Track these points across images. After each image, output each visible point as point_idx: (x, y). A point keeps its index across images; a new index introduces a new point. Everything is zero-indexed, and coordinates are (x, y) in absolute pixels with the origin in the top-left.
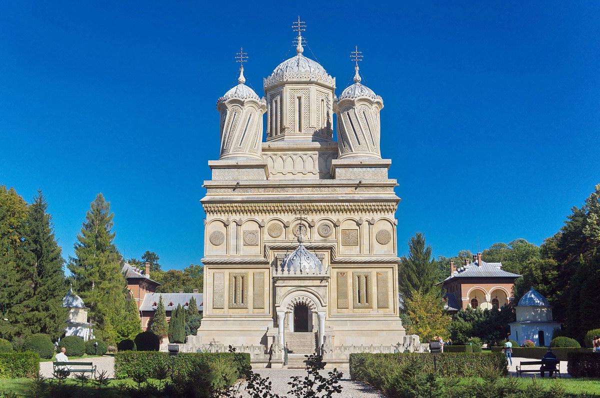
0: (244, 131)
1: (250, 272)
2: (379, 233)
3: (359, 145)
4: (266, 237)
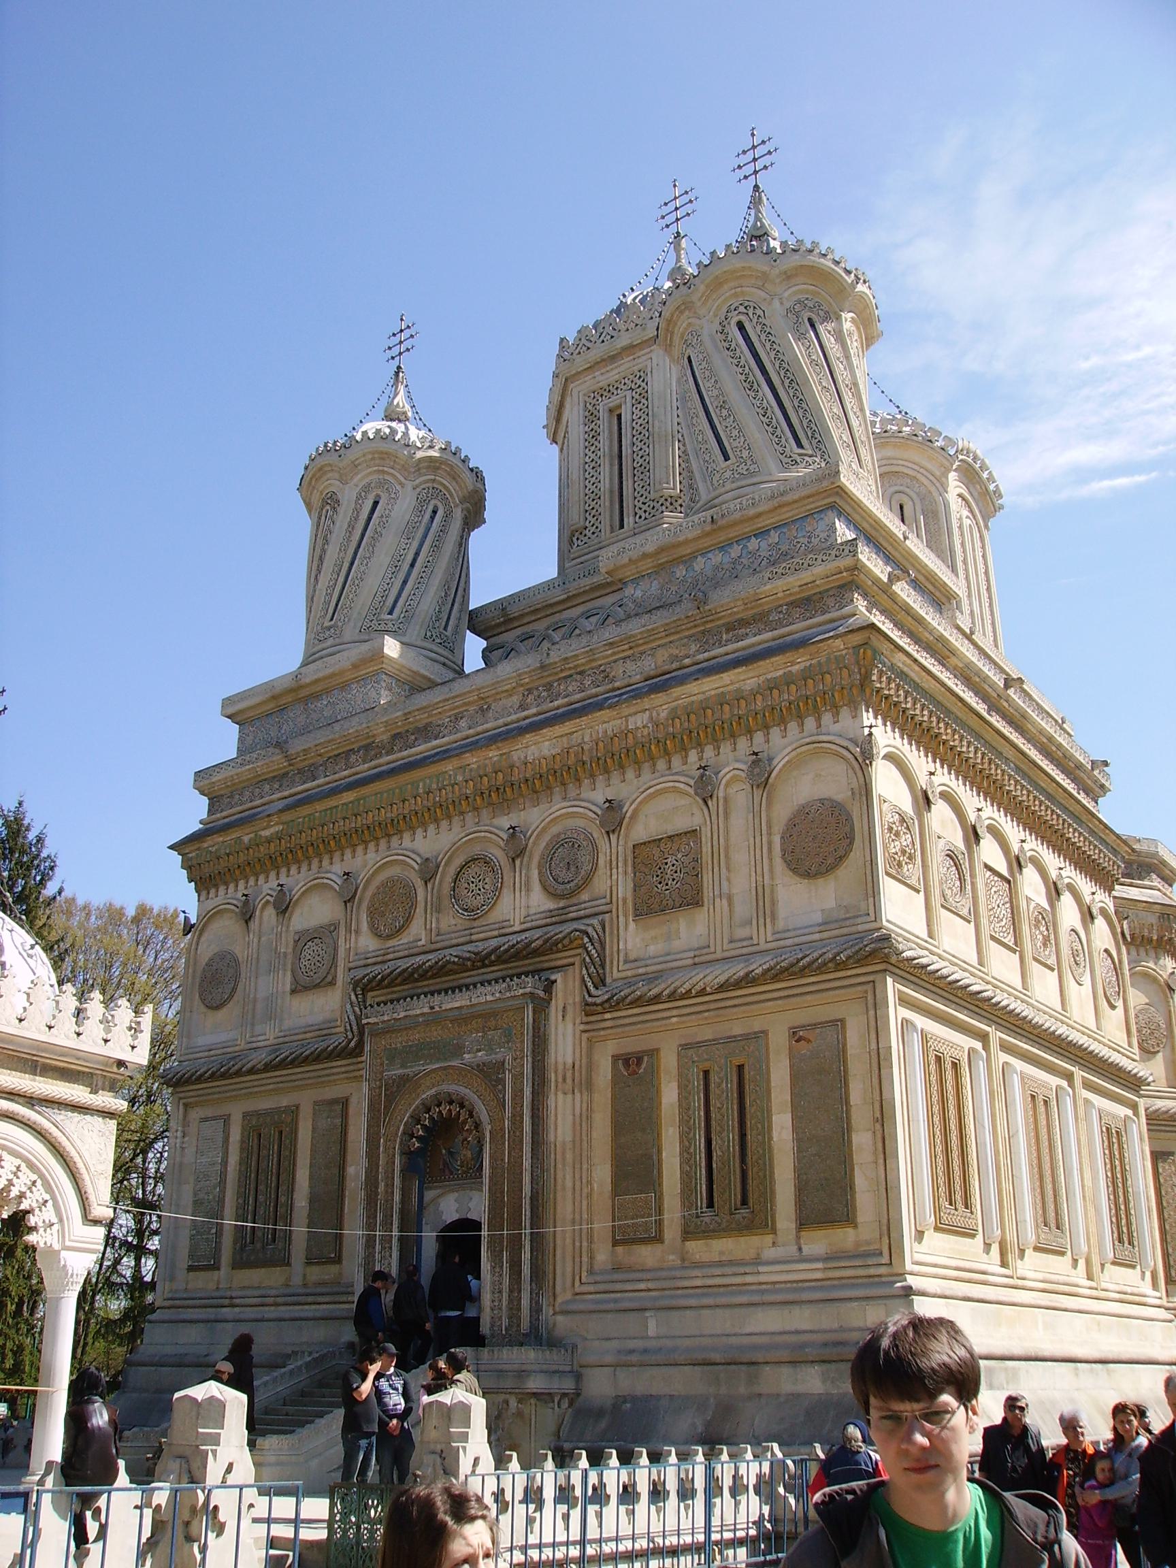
1: (306, 1100)
2: (792, 824)
3: (726, 458)
4: (367, 942)
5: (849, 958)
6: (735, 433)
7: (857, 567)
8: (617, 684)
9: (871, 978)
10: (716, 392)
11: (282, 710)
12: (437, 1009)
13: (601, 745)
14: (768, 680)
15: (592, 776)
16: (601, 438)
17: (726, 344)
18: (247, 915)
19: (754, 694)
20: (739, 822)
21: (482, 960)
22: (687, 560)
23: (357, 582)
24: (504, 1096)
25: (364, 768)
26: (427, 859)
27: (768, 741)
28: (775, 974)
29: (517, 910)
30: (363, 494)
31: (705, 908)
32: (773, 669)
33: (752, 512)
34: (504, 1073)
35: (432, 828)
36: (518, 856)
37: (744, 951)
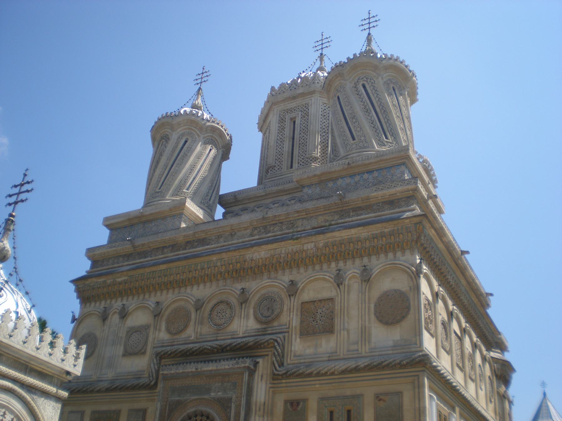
0: (169, 166)
3: (354, 139)
4: (163, 335)
5: (407, 363)
6: (359, 129)
7: (416, 190)
8: (299, 229)
9: (417, 373)
10: (350, 112)
11: (132, 225)
12: (199, 370)
13: (289, 255)
14: (373, 234)
15: (284, 269)
16: (286, 130)
17: (357, 92)
18: (104, 318)
19: (366, 239)
20: (354, 296)
21: (222, 350)
22: (334, 180)
23: (173, 174)
24: (230, 415)
25: (171, 255)
26: (199, 300)
27: (370, 261)
28: (370, 368)
29: (242, 328)
30: (181, 137)
31: (335, 334)
32: (375, 229)
33: (367, 162)
34: (231, 404)
35: (202, 286)
36: (244, 302)
37: (354, 356)
